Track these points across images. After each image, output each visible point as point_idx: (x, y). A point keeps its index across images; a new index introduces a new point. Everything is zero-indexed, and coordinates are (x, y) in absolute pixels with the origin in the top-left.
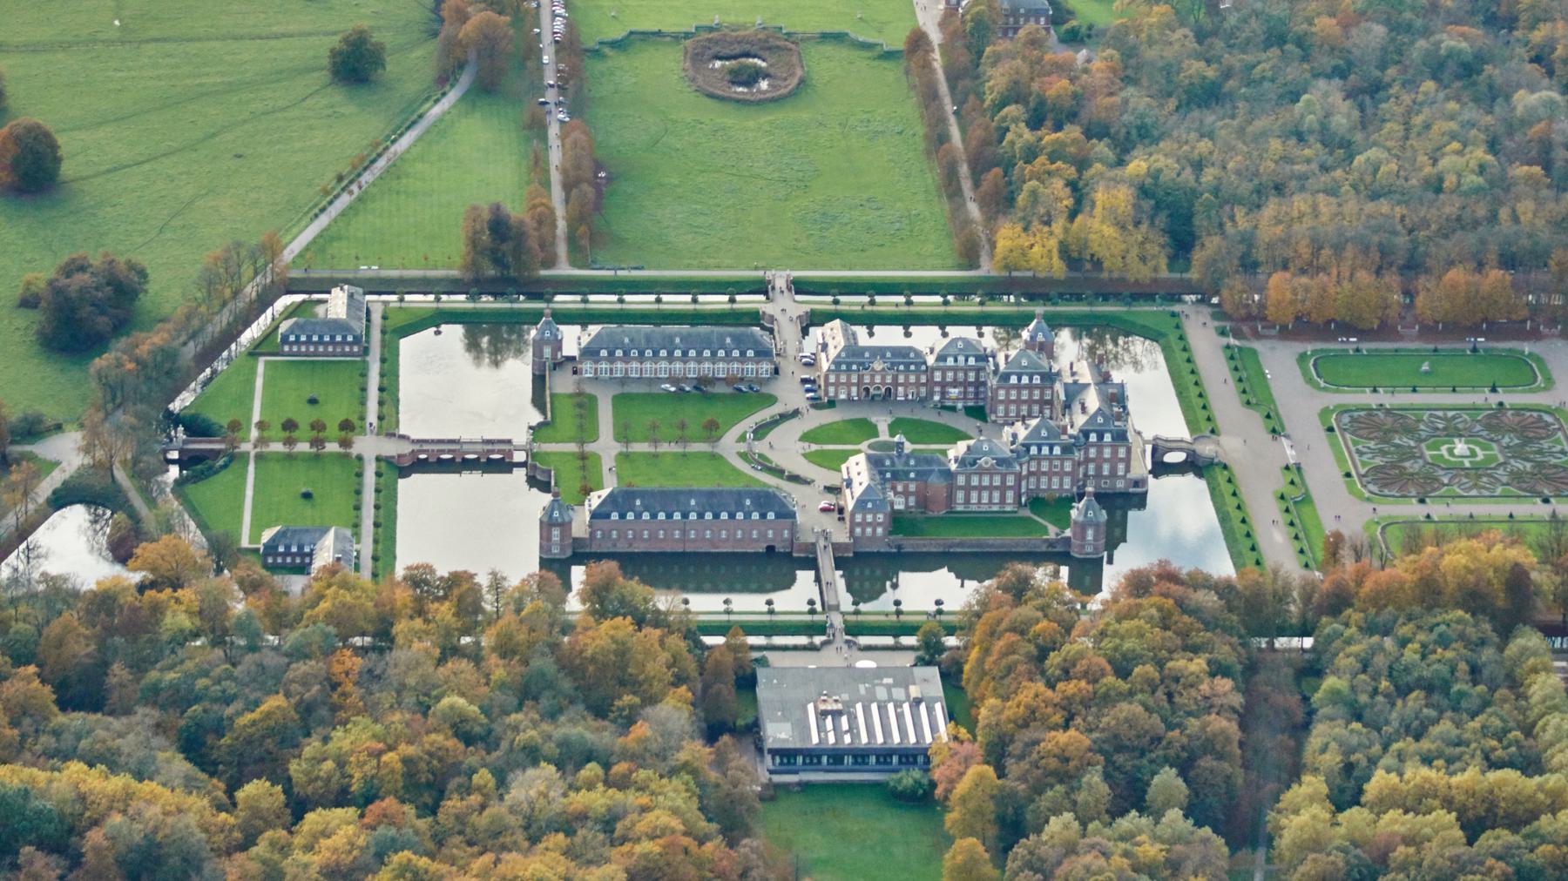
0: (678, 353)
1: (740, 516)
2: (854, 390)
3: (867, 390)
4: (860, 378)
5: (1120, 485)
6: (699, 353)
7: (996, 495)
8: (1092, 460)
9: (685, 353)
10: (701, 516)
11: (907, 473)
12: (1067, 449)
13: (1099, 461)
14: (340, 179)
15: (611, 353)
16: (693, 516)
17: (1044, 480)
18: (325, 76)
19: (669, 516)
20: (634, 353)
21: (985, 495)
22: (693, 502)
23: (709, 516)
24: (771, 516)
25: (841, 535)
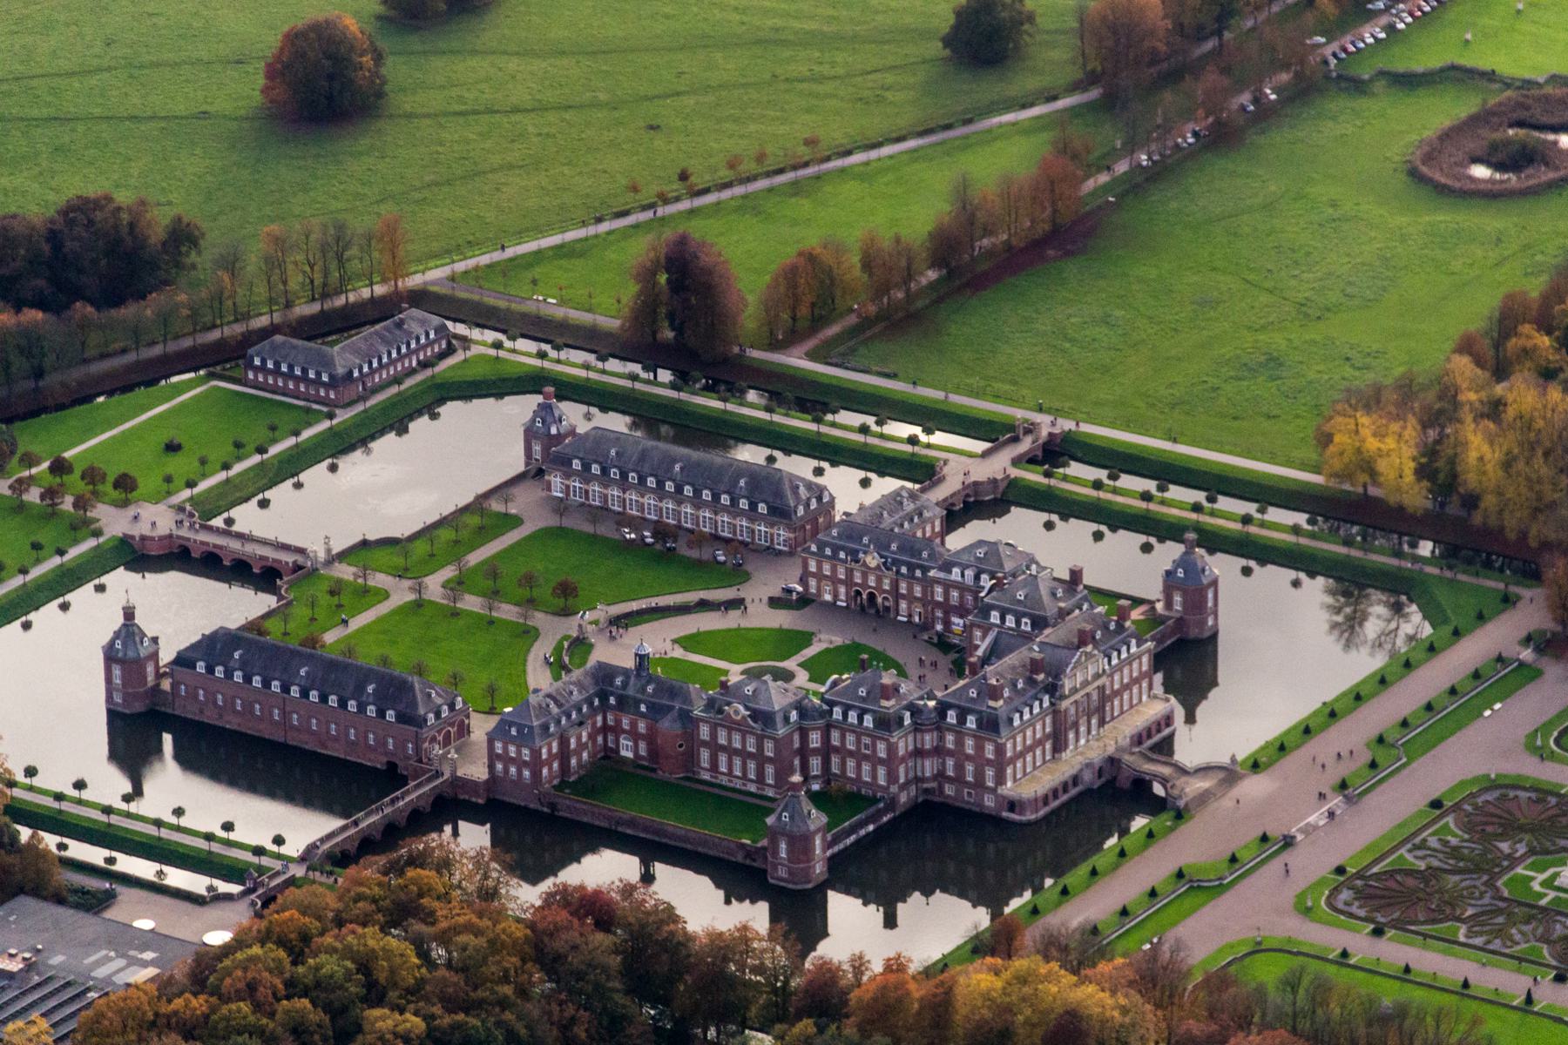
0: (669, 486)
1: (352, 705)
2: (842, 590)
3: (858, 593)
4: (850, 572)
5: (989, 802)
6: (697, 493)
7: (752, 765)
8: (950, 753)
9: (679, 489)
10: (305, 694)
11: (638, 702)
12: (886, 723)
13: (959, 754)
14: (684, 176)
15: (586, 467)
16: (295, 691)
17: (851, 763)
18: (936, 49)
19: (266, 684)
20: (614, 473)
21: (737, 762)
22: (303, 672)
23: (314, 696)
24: (390, 715)
25: (477, 771)
